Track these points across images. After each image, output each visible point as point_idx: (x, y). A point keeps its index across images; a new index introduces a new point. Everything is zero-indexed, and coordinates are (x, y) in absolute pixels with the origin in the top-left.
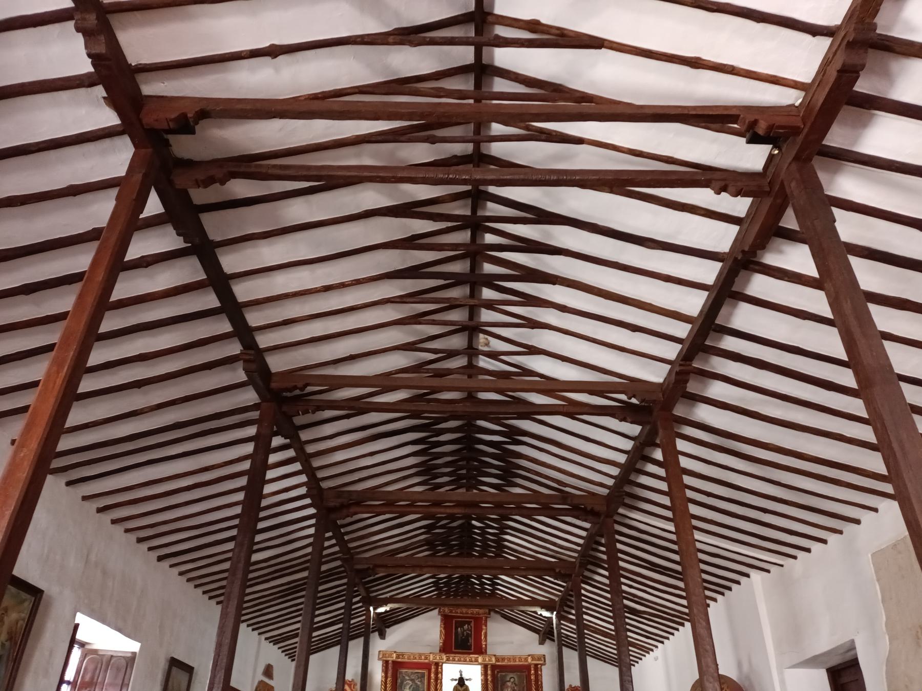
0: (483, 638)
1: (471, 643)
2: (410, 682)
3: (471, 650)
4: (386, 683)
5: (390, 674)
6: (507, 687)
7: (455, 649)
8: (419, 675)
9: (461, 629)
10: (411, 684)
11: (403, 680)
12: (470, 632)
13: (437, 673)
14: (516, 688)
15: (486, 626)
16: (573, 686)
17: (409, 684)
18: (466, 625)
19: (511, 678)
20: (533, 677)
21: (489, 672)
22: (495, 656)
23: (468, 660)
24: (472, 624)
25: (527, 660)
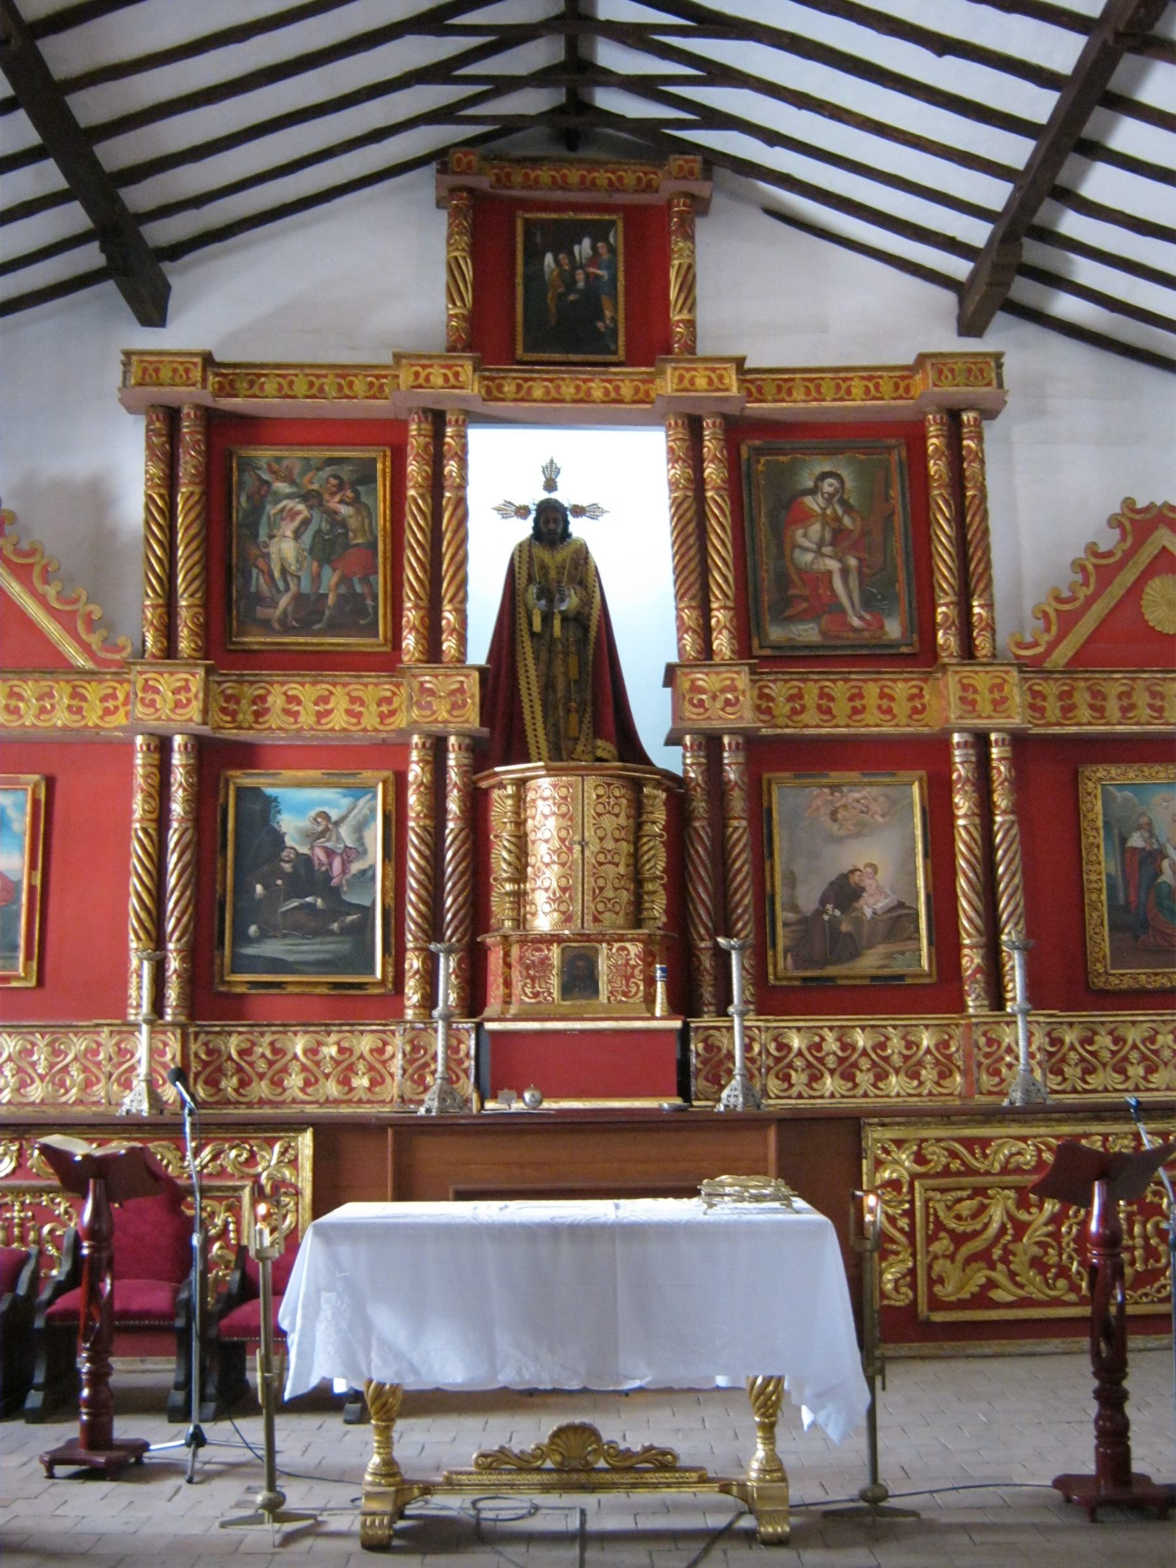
0: (673, 295)
1: (614, 320)
2: (301, 507)
3: (615, 352)
4: (170, 512)
5: (189, 463)
6: (806, 517)
7: (527, 349)
8: (346, 472)
9: (556, 260)
10: (306, 513)
11: (262, 495)
12: (603, 273)
13: (437, 460)
14: (847, 521)
15: (690, 238)
16: (1140, 505)
17: (293, 514)
18: (586, 242)
19: (824, 476)
20: (936, 467)
21: (710, 446)
22: (740, 362)
23: (598, 394)
24: (617, 237)
25: (907, 389)
